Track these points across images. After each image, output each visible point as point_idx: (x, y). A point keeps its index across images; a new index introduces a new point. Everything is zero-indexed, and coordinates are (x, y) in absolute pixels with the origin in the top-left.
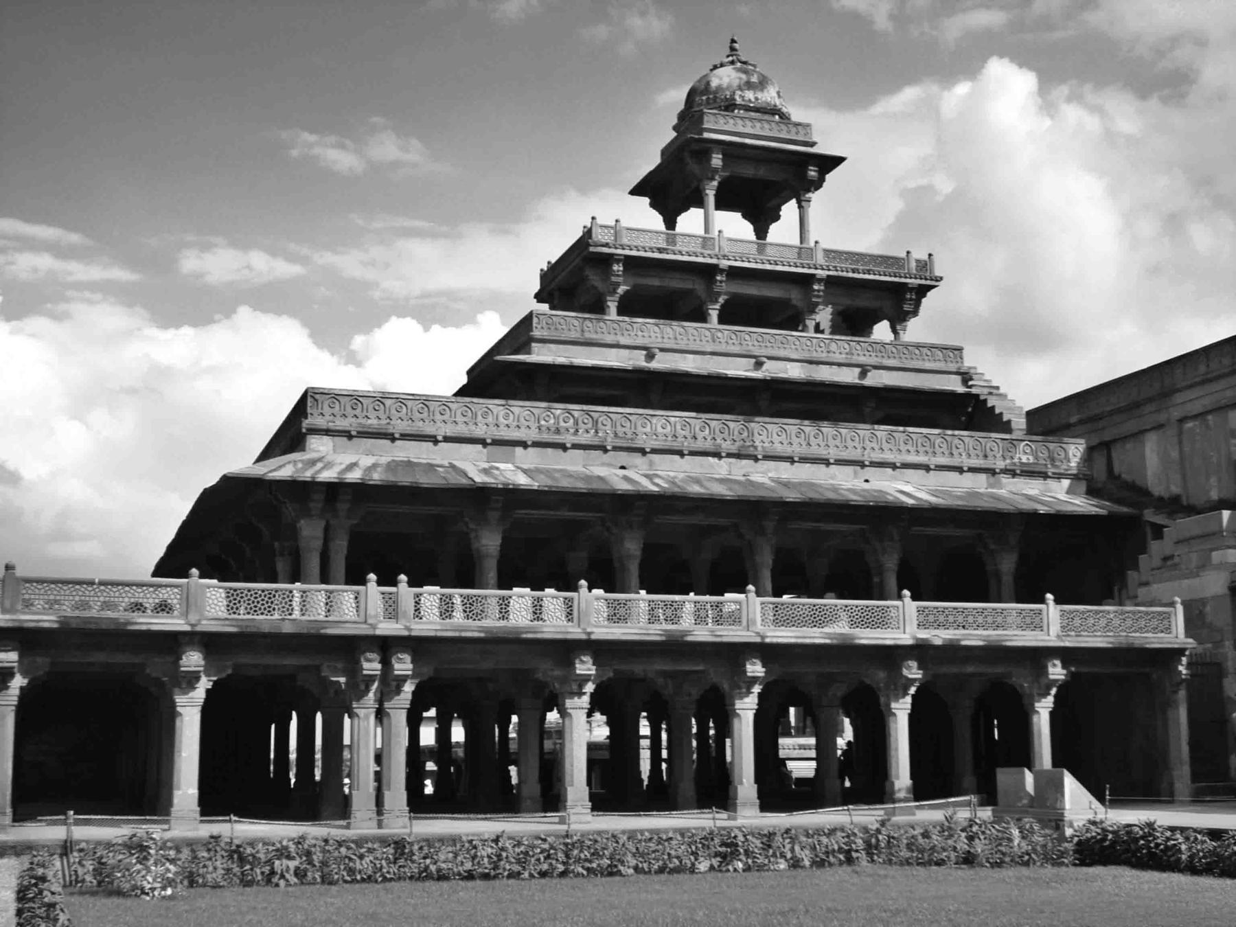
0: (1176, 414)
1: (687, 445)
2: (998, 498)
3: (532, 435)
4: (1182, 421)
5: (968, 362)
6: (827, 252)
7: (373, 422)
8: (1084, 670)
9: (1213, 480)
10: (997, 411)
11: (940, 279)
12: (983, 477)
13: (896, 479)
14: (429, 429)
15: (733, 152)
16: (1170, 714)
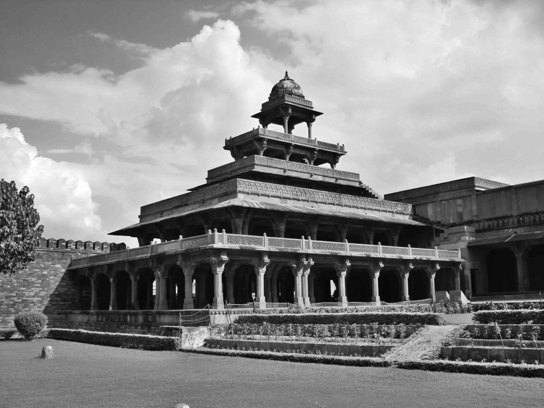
0: (439, 199)
1: (328, 201)
2: (394, 219)
3: (292, 197)
4: (441, 201)
5: (361, 179)
6: (318, 142)
7: (253, 190)
9: (451, 217)
10: (373, 194)
11: (346, 152)
12: (391, 214)
13: (372, 213)
14: (267, 193)
16: (456, 279)
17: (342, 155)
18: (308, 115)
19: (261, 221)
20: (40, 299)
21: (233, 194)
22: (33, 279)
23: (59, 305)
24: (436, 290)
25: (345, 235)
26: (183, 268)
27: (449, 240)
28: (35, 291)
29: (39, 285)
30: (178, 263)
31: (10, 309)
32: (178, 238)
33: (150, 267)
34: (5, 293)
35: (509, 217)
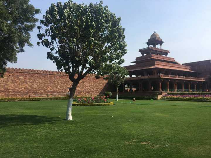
18: (161, 43)
19: (160, 71)
21: (154, 64)
24: (184, 89)
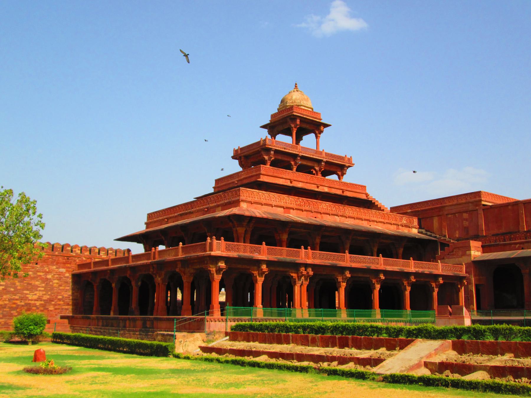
0: (446, 213)
1: (331, 212)
2: (399, 232)
3: (295, 207)
5: (368, 191)
6: (326, 153)
7: (256, 199)
8: (447, 281)
9: (457, 232)
12: (395, 226)
13: (376, 225)
14: (270, 203)
15: (304, 120)
16: (460, 294)
17: (349, 166)
18: (315, 127)
20: (43, 302)
21: (236, 203)
22: (37, 283)
23: (63, 309)
25: (348, 246)
26: (182, 274)
27: (453, 255)
28: (38, 294)
29: (43, 289)
30: (177, 270)
31: (12, 312)
32: (178, 245)
33: (150, 273)
34: (8, 296)
35: (516, 232)
